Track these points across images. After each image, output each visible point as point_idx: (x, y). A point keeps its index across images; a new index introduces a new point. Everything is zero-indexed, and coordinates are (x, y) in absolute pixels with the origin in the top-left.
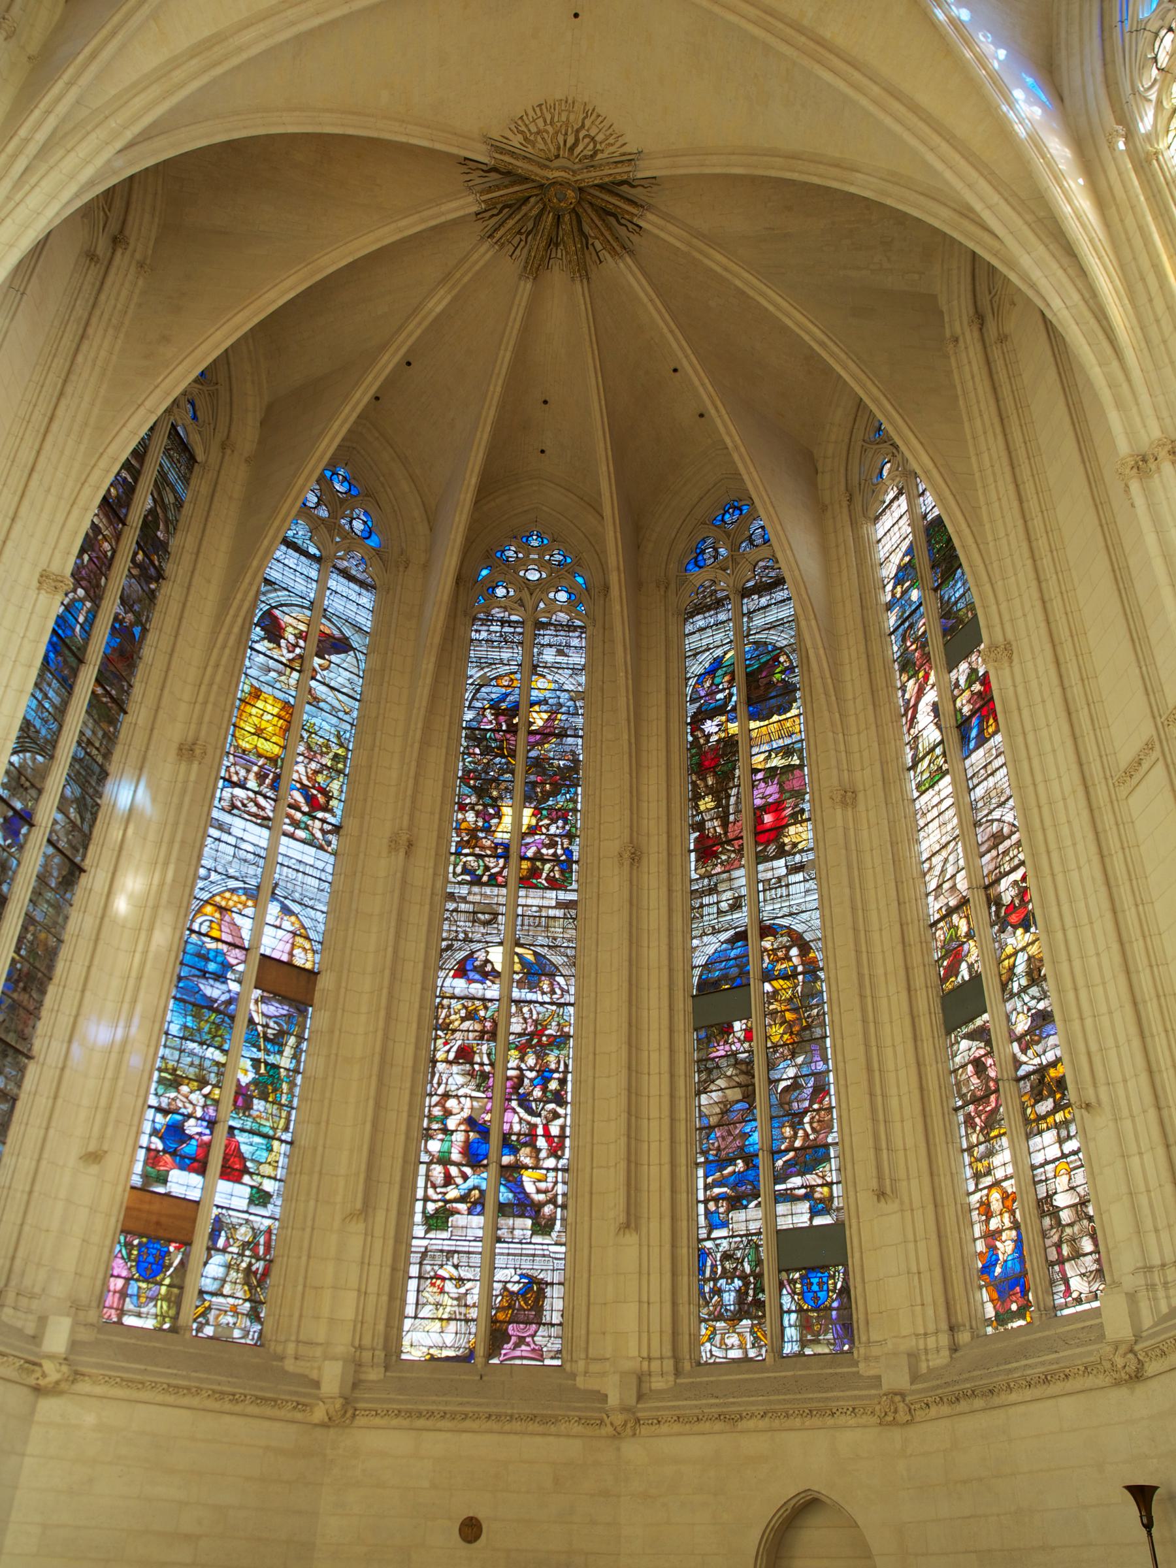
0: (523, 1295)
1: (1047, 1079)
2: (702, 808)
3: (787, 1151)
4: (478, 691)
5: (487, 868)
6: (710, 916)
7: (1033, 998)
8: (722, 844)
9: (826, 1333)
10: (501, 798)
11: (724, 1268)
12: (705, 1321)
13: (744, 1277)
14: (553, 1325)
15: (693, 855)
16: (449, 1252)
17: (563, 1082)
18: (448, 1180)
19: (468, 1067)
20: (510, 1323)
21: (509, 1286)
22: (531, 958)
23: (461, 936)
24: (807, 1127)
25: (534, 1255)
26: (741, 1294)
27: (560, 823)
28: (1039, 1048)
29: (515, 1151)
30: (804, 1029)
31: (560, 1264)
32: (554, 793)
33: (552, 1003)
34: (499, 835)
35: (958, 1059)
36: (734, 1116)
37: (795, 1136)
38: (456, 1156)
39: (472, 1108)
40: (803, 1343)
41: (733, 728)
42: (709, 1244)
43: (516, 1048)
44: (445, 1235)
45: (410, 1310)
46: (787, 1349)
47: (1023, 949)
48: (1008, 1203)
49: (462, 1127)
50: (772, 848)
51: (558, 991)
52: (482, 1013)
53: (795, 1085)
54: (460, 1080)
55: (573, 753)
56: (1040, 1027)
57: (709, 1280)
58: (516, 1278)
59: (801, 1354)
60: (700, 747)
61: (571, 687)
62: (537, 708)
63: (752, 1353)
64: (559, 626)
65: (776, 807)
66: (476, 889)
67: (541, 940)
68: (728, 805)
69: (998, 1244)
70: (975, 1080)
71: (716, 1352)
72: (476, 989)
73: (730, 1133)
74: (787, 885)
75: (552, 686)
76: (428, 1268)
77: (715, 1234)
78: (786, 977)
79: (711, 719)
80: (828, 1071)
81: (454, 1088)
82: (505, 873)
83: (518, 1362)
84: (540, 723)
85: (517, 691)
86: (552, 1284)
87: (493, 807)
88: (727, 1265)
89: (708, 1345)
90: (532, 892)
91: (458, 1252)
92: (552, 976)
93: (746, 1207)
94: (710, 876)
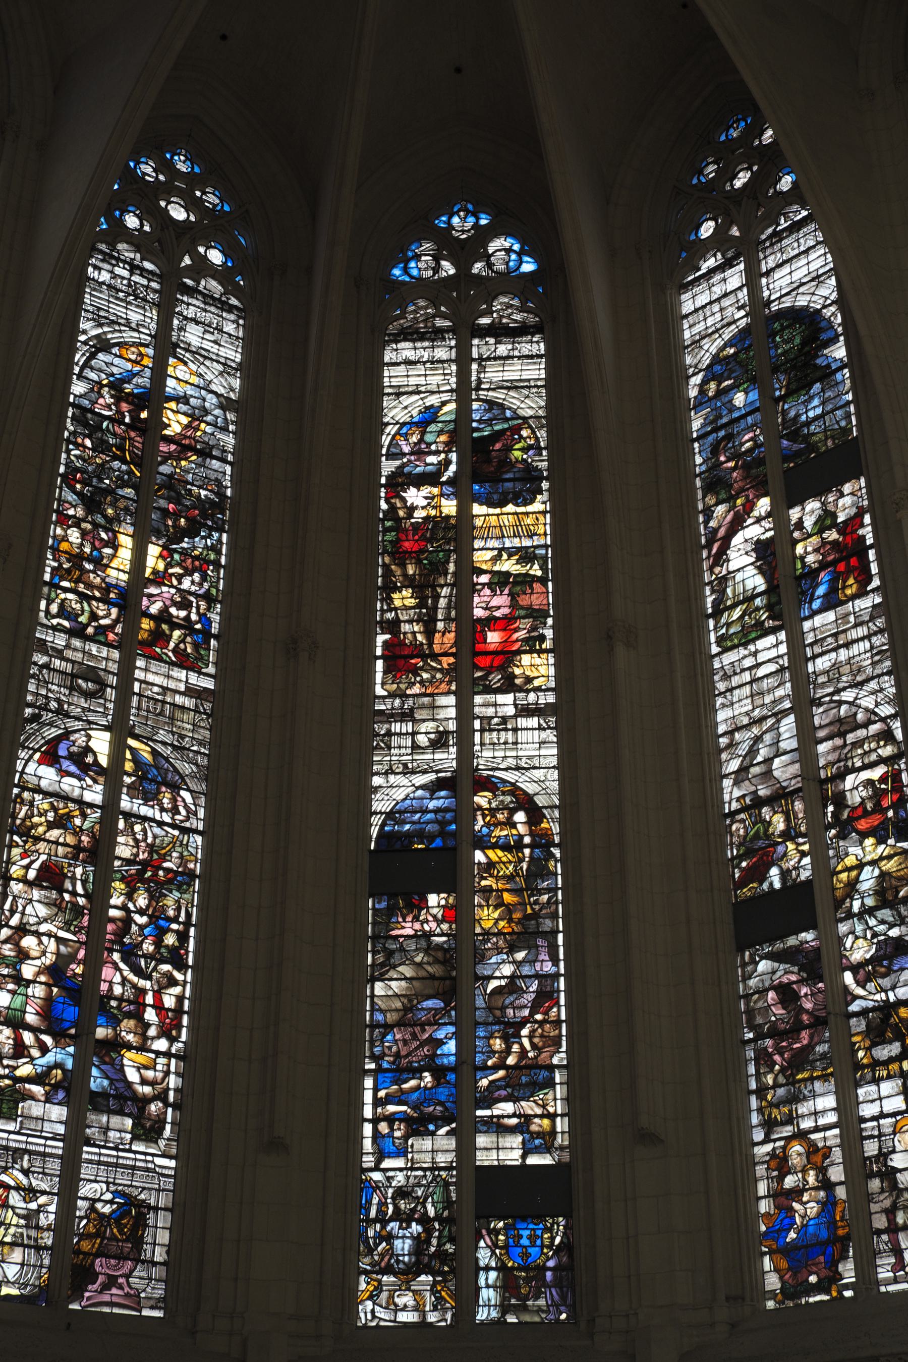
0: (118, 1222)
1: (894, 1019)
2: (398, 603)
3: (495, 1068)
4: (93, 356)
5: (94, 617)
6: (400, 752)
7: (882, 922)
8: (424, 657)
9: (537, 1298)
10: (118, 520)
11: (396, 1207)
12: (366, 1273)
13: (424, 1220)
14: (155, 1264)
15: (380, 665)
16: (16, 1150)
17: (183, 937)
18: (20, 1050)
19: (54, 894)
20: (97, 1255)
21: (99, 1205)
22: (147, 756)
23: (53, 705)
24: (526, 1042)
25: (133, 1168)
26: (420, 1243)
27: (197, 577)
28: (886, 982)
29: (114, 1021)
30: (527, 917)
31: (169, 1184)
32: (192, 531)
33: (173, 826)
34: (110, 571)
35: (752, 982)
36: (422, 1016)
37: (508, 1052)
38: (31, 1019)
39: (58, 954)
40: (505, 1309)
41: (449, 507)
42: (377, 1176)
43: (122, 880)
44: (11, 1127)
46: (482, 1315)
47: (873, 863)
48: (817, 1158)
49: (43, 978)
50: (496, 678)
51: (183, 812)
52: (78, 822)
53: (513, 986)
54: (42, 911)
55: (219, 483)
56: (891, 958)
57: (375, 1221)
58: (108, 1196)
59: (500, 1323)
60: (398, 520)
61: (221, 390)
62: (173, 405)
63: (432, 1318)
64: (208, 299)
65: (506, 624)
66: (77, 643)
67: (162, 735)
68: (435, 608)
69: (796, 1205)
70: (779, 1011)
71: (381, 1313)
72: (70, 785)
73: (414, 1036)
74: (515, 730)
75: (195, 380)
77: (387, 1164)
78: (506, 848)
79: (418, 486)
80: (557, 975)
81: (33, 920)
82: (119, 629)
83: (107, 1310)
84: (177, 429)
85: (148, 373)
86: (156, 1209)
87: (107, 530)
88: (402, 1204)
89: (369, 1304)
90: (154, 665)
92: (175, 788)
93: (433, 1134)
94: (404, 696)
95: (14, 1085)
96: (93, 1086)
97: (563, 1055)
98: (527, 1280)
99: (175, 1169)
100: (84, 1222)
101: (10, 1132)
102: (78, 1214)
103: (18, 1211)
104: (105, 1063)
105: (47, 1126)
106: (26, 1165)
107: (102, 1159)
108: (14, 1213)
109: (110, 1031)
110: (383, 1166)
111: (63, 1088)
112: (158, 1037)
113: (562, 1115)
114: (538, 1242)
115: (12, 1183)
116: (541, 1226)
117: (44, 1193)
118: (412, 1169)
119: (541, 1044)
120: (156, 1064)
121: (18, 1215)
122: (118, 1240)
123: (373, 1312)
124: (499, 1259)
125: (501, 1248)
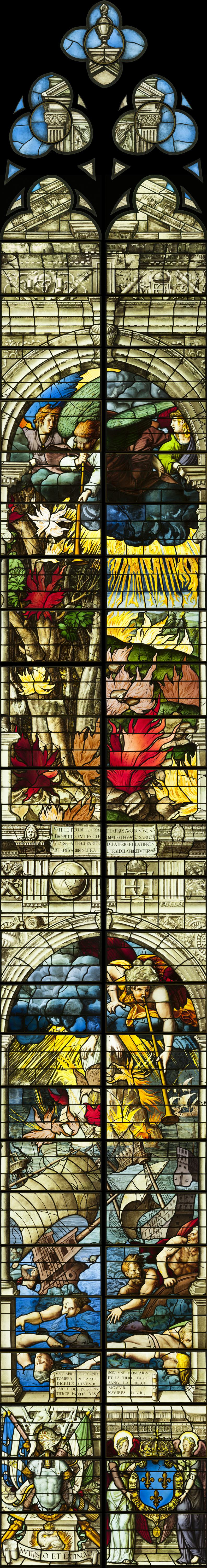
57: (17, 1458)
73: (55, 1259)
97: (203, 1284)
98: (160, 1525)
110: (24, 1400)
113: (198, 1350)
114: (170, 1485)
116: (173, 1469)
118: (54, 1404)
119: (178, 1271)
123: (18, 1550)
124: (131, 1502)
125: (132, 1491)
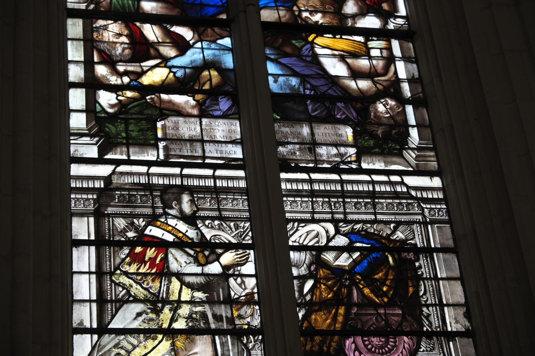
0: (368, 277)
14: (451, 336)
20: (348, 331)
21: (329, 256)
25: (373, 195)
44: (151, 156)
45: (84, 315)
58: (341, 241)
76: (121, 223)
86: (428, 251)
91: (192, 190)
95: (143, 97)
96: (274, 86)
99: (443, 189)
100: (309, 284)
101: (149, 164)
102: (295, 272)
103: (188, 279)
104: (286, 55)
105: (211, 150)
106: (187, 208)
107: (316, 187)
108: (183, 283)
109: (282, 13)
111: (226, 94)
112: (362, 14)
115: (170, 238)
117: (228, 247)
120: (369, 49)
121: (192, 287)
122: (376, 306)
